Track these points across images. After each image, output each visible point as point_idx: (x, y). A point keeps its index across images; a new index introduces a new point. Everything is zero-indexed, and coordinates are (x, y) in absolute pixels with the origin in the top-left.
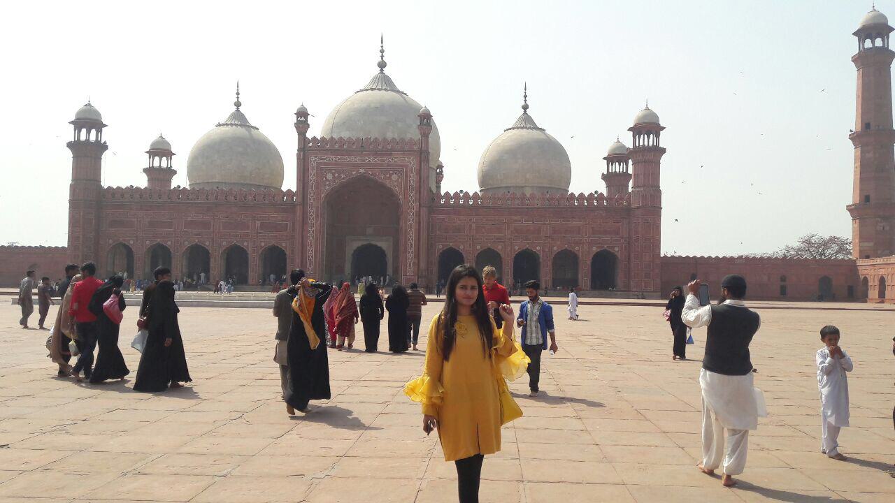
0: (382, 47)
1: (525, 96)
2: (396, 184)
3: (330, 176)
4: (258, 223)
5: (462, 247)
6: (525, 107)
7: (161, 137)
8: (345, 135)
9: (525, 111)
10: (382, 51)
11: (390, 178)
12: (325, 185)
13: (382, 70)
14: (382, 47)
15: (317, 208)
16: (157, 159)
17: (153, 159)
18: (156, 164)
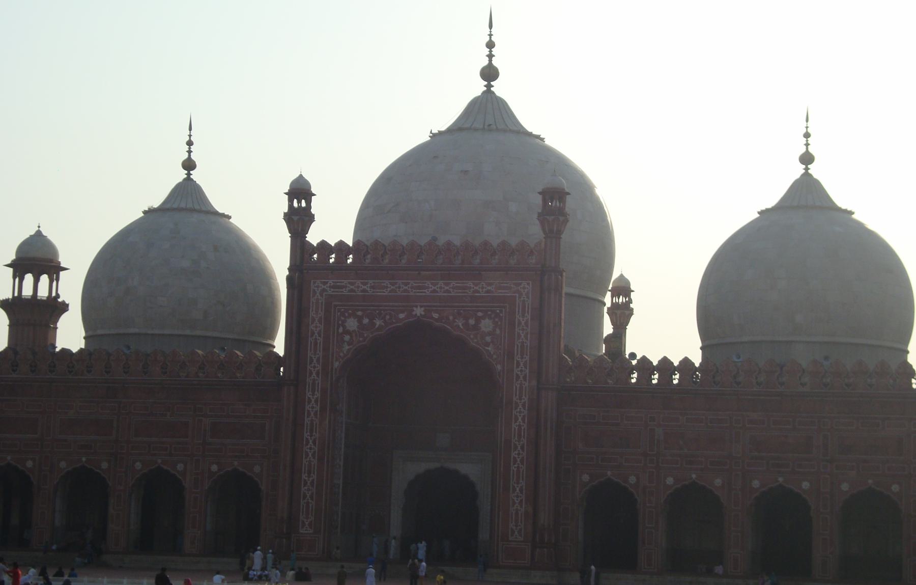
0: (490, 35)
1: (807, 135)
2: (488, 339)
3: (352, 324)
5: (632, 480)
6: (807, 159)
7: (39, 234)
8: (396, 231)
9: (807, 169)
10: (490, 45)
11: (476, 327)
13: (489, 86)
14: (490, 35)
16: (29, 278)
17: (21, 280)
18: (27, 291)
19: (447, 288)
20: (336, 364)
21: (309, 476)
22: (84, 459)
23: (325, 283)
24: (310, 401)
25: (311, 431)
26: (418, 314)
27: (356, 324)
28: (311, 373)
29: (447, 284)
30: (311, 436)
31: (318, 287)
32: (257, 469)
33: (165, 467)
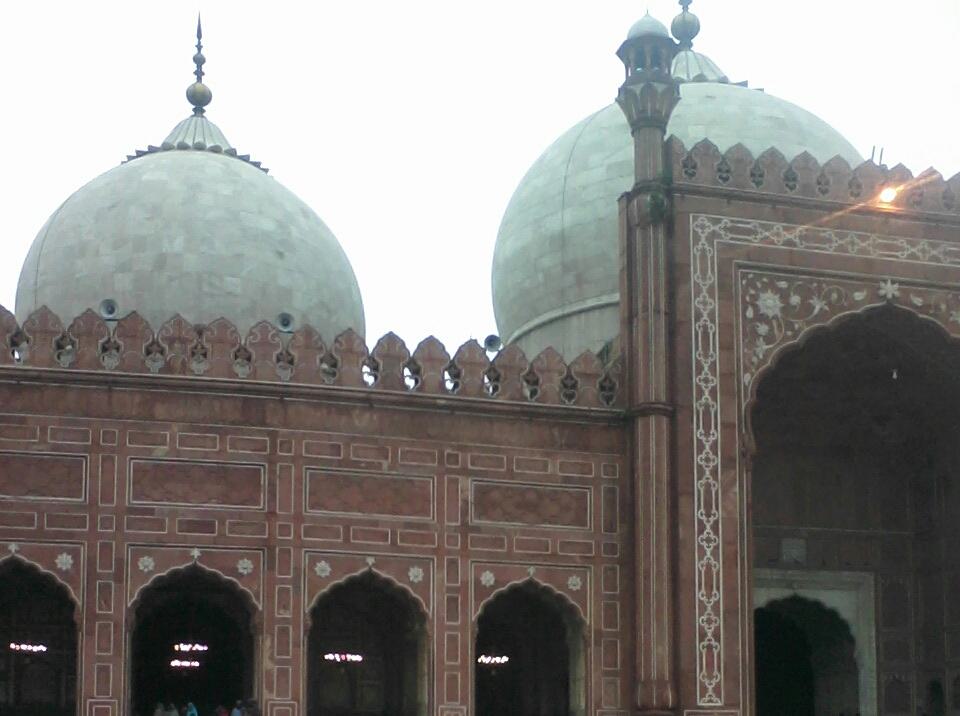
3: (770, 303)
4: (468, 486)
12: (752, 336)
15: (727, 426)
19: (934, 252)
20: (747, 378)
21: (709, 596)
22: (196, 553)
23: (717, 222)
24: (701, 448)
25: (708, 506)
26: (890, 296)
27: (779, 304)
28: (700, 393)
29: (934, 246)
30: (708, 515)
31: (703, 227)
32: (574, 583)
33: (384, 575)
